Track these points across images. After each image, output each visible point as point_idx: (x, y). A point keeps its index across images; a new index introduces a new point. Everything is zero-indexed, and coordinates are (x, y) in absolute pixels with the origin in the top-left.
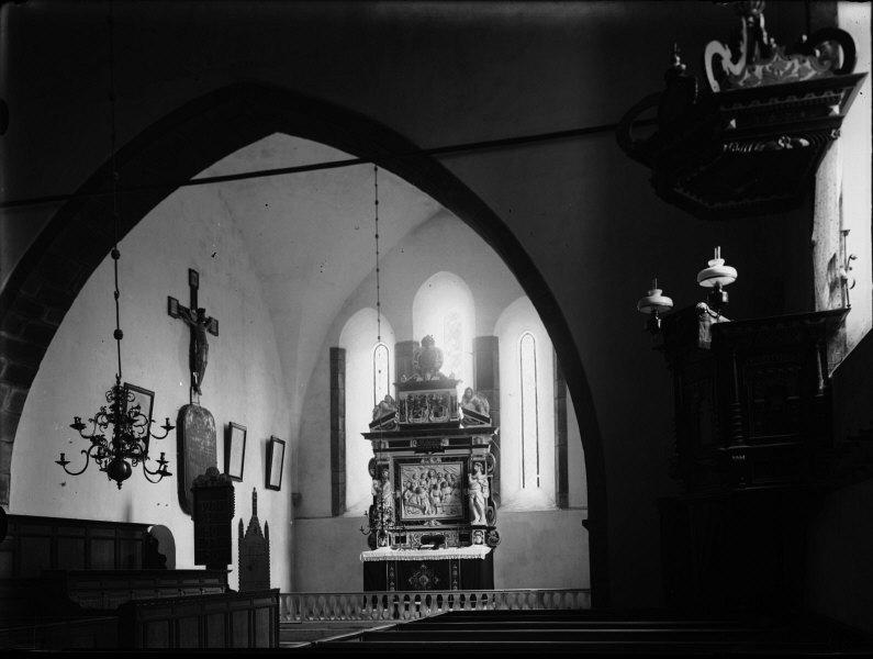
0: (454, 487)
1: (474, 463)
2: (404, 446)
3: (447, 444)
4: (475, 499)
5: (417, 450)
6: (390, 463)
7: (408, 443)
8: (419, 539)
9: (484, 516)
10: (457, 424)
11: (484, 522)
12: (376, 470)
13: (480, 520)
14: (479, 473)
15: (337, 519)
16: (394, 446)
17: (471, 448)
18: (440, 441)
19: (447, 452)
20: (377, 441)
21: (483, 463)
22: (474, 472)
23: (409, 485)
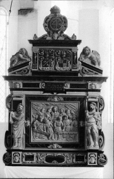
0: (73, 120)
23: (37, 117)
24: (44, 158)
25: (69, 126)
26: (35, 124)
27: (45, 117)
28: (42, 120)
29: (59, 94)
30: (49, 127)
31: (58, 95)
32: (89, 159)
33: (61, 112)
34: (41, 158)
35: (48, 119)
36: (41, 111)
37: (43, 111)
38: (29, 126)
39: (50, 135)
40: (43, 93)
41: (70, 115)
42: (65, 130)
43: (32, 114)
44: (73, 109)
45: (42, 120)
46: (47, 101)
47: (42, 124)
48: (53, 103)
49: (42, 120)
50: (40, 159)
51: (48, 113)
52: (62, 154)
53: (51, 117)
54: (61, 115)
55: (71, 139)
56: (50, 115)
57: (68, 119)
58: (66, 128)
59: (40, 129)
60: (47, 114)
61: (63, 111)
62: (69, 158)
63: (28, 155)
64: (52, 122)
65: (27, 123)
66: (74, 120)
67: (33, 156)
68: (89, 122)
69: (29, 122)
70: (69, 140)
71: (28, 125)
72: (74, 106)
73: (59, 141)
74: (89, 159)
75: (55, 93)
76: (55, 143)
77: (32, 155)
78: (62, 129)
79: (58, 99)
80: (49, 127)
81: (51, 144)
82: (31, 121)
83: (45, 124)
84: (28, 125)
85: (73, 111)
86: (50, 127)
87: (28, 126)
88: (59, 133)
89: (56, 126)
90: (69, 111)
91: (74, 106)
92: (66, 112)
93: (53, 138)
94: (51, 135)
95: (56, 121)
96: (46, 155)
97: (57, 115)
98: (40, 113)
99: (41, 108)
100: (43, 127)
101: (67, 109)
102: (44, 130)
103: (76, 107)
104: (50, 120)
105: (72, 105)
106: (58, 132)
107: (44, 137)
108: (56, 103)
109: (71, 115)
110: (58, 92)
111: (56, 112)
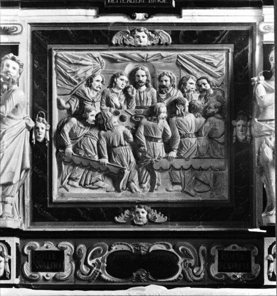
0: (206, 116)
23: (75, 105)
24: (103, 260)
25: (193, 140)
26: (67, 133)
27: (105, 107)
28: (91, 119)
29: (155, 19)
30: (121, 145)
31: (150, 20)
32: (270, 262)
33: (164, 87)
34: (90, 263)
35: (116, 113)
36: (89, 82)
37: (97, 84)
38: (45, 139)
39: (121, 172)
40: (97, 16)
41: (195, 96)
42: (178, 154)
43: (55, 96)
44: (206, 75)
45: (91, 119)
46: (111, 44)
47: (95, 132)
48: (134, 54)
49: (93, 118)
50: (86, 263)
51: (115, 90)
52: (168, 247)
53: (125, 107)
54: (163, 96)
55: (204, 188)
56: (123, 97)
57: (190, 111)
58: (181, 146)
59: (86, 151)
60: (111, 95)
61: (169, 83)
62: (193, 262)
63: (43, 249)
64: (131, 125)
65: (37, 128)
66: (213, 114)
67: (60, 254)
68: (267, 121)
69: (44, 126)
70: (192, 192)
71: (42, 137)
72: (211, 64)
73: (154, 197)
74: (270, 262)
75: (140, 16)
76: (141, 204)
77: (56, 249)
78: (168, 148)
79: (150, 38)
80: (121, 145)
81: (125, 209)
82: (51, 123)
83: (103, 132)
84: (42, 137)
85: (209, 82)
86: (123, 142)
87: (41, 140)
88: (155, 166)
89: (143, 140)
90: (191, 80)
91: (211, 64)
92: (182, 85)
93: (135, 185)
94: (127, 172)
95: (145, 121)
96: (110, 249)
97: (150, 98)
98: (86, 89)
99: (89, 74)
100: (98, 144)
101: (184, 74)
102: (101, 156)
103: (219, 69)
104: (122, 119)
105: (203, 60)
106: (151, 164)
107: (101, 183)
108: (143, 54)
109: (200, 97)
110: (151, 13)
111: (144, 88)
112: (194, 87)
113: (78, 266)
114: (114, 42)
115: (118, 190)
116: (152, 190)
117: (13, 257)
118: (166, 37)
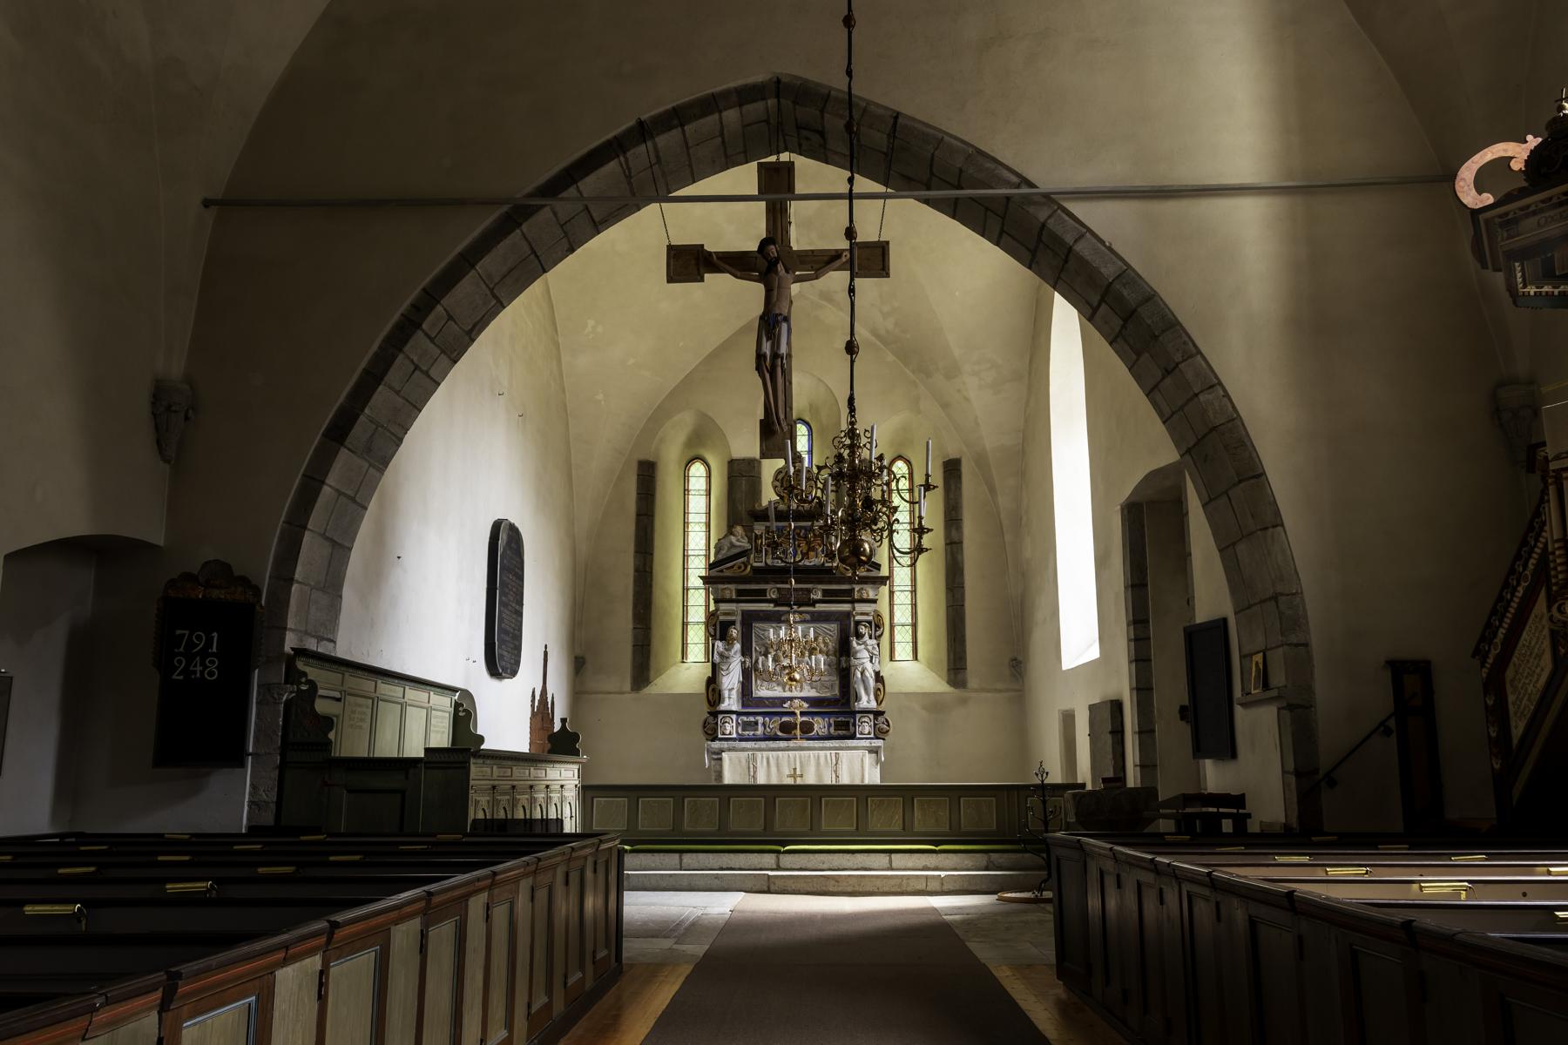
1: (858, 623)
2: (759, 596)
3: (819, 596)
4: (862, 673)
5: (776, 602)
6: (738, 619)
7: (763, 592)
8: (777, 725)
9: (872, 697)
10: (830, 570)
11: (873, 705)
12: (718, 628)
13: (866, 701)
14: (866, 637)
15: (634, 695)
16: (743, 596)
17: (853, 602)
18: (809, 591)
19: (820, 607)
20: (721, 586)
21: (870, 623)
22: (859, 636)
23: (763, 650)
29: (802, 609)
41: (822, 646)
67: (756, 723)
72: (830, 630)
76: (796, 698)
82: (751, 658)
91: (830, 630)
112: (821, 641)
113: (765, 728)
114: (783, 619)
115: (784, 691)
116: (801, 691)
117: (734, 724)
118: (808, 617)
